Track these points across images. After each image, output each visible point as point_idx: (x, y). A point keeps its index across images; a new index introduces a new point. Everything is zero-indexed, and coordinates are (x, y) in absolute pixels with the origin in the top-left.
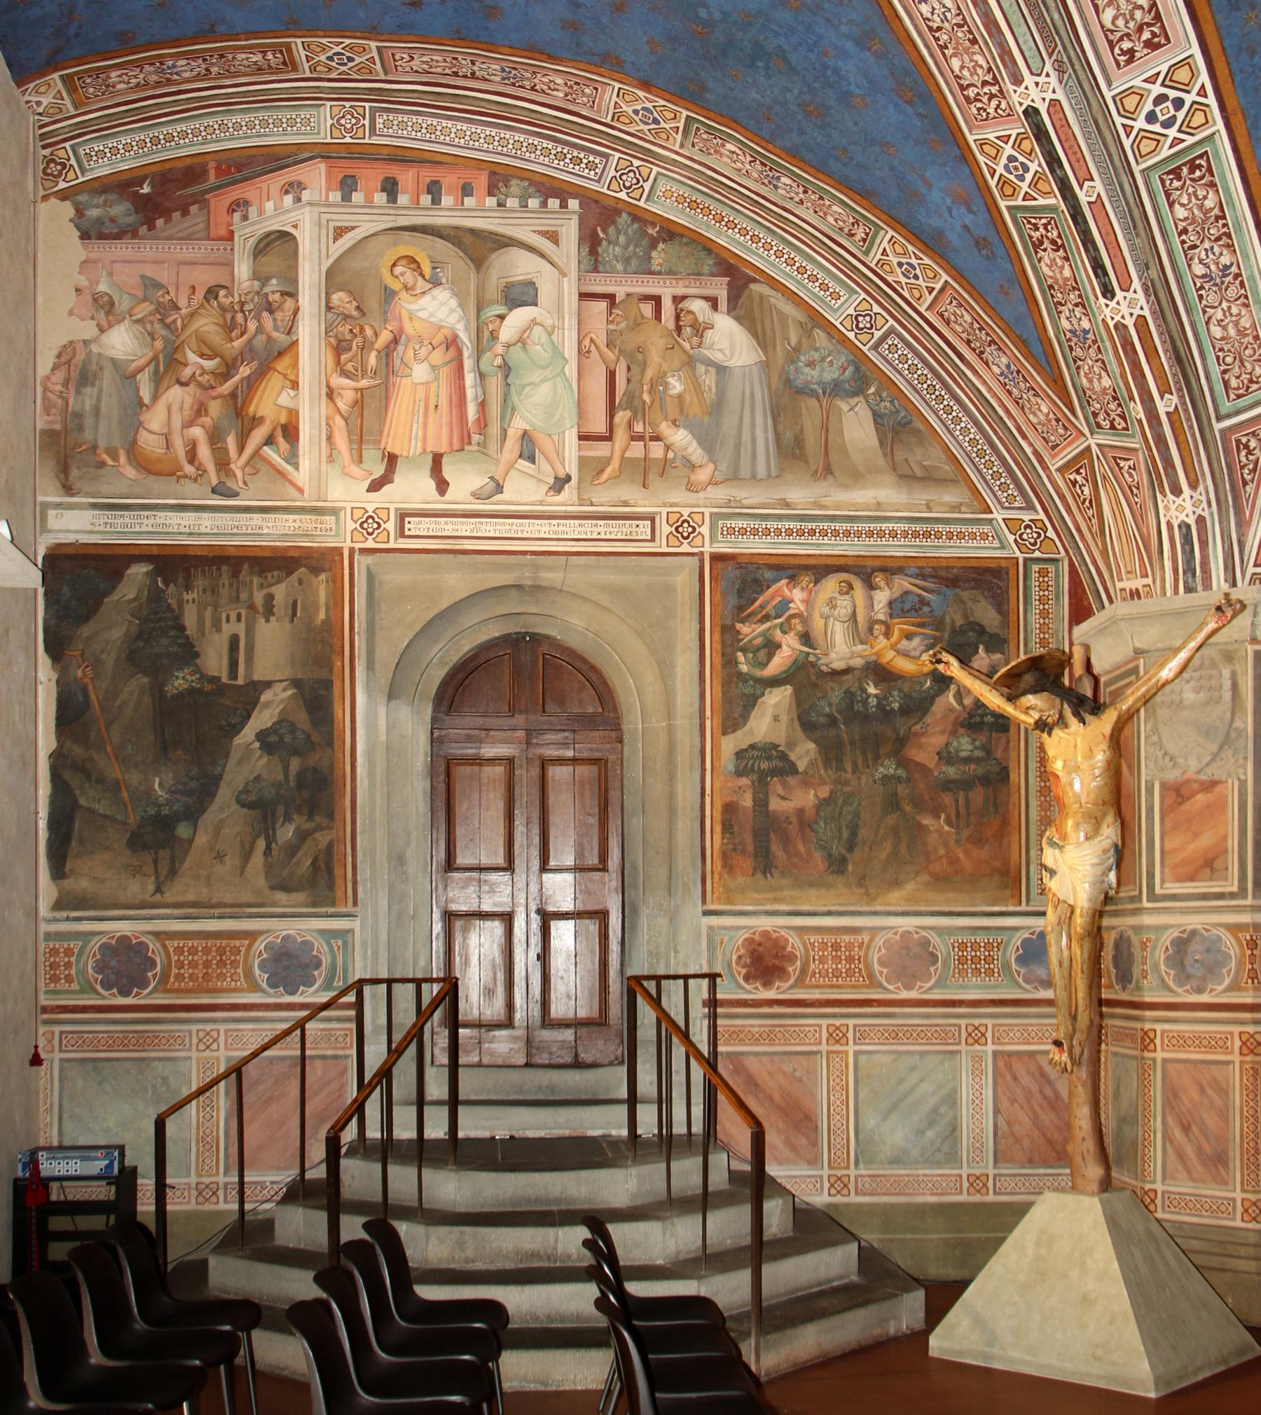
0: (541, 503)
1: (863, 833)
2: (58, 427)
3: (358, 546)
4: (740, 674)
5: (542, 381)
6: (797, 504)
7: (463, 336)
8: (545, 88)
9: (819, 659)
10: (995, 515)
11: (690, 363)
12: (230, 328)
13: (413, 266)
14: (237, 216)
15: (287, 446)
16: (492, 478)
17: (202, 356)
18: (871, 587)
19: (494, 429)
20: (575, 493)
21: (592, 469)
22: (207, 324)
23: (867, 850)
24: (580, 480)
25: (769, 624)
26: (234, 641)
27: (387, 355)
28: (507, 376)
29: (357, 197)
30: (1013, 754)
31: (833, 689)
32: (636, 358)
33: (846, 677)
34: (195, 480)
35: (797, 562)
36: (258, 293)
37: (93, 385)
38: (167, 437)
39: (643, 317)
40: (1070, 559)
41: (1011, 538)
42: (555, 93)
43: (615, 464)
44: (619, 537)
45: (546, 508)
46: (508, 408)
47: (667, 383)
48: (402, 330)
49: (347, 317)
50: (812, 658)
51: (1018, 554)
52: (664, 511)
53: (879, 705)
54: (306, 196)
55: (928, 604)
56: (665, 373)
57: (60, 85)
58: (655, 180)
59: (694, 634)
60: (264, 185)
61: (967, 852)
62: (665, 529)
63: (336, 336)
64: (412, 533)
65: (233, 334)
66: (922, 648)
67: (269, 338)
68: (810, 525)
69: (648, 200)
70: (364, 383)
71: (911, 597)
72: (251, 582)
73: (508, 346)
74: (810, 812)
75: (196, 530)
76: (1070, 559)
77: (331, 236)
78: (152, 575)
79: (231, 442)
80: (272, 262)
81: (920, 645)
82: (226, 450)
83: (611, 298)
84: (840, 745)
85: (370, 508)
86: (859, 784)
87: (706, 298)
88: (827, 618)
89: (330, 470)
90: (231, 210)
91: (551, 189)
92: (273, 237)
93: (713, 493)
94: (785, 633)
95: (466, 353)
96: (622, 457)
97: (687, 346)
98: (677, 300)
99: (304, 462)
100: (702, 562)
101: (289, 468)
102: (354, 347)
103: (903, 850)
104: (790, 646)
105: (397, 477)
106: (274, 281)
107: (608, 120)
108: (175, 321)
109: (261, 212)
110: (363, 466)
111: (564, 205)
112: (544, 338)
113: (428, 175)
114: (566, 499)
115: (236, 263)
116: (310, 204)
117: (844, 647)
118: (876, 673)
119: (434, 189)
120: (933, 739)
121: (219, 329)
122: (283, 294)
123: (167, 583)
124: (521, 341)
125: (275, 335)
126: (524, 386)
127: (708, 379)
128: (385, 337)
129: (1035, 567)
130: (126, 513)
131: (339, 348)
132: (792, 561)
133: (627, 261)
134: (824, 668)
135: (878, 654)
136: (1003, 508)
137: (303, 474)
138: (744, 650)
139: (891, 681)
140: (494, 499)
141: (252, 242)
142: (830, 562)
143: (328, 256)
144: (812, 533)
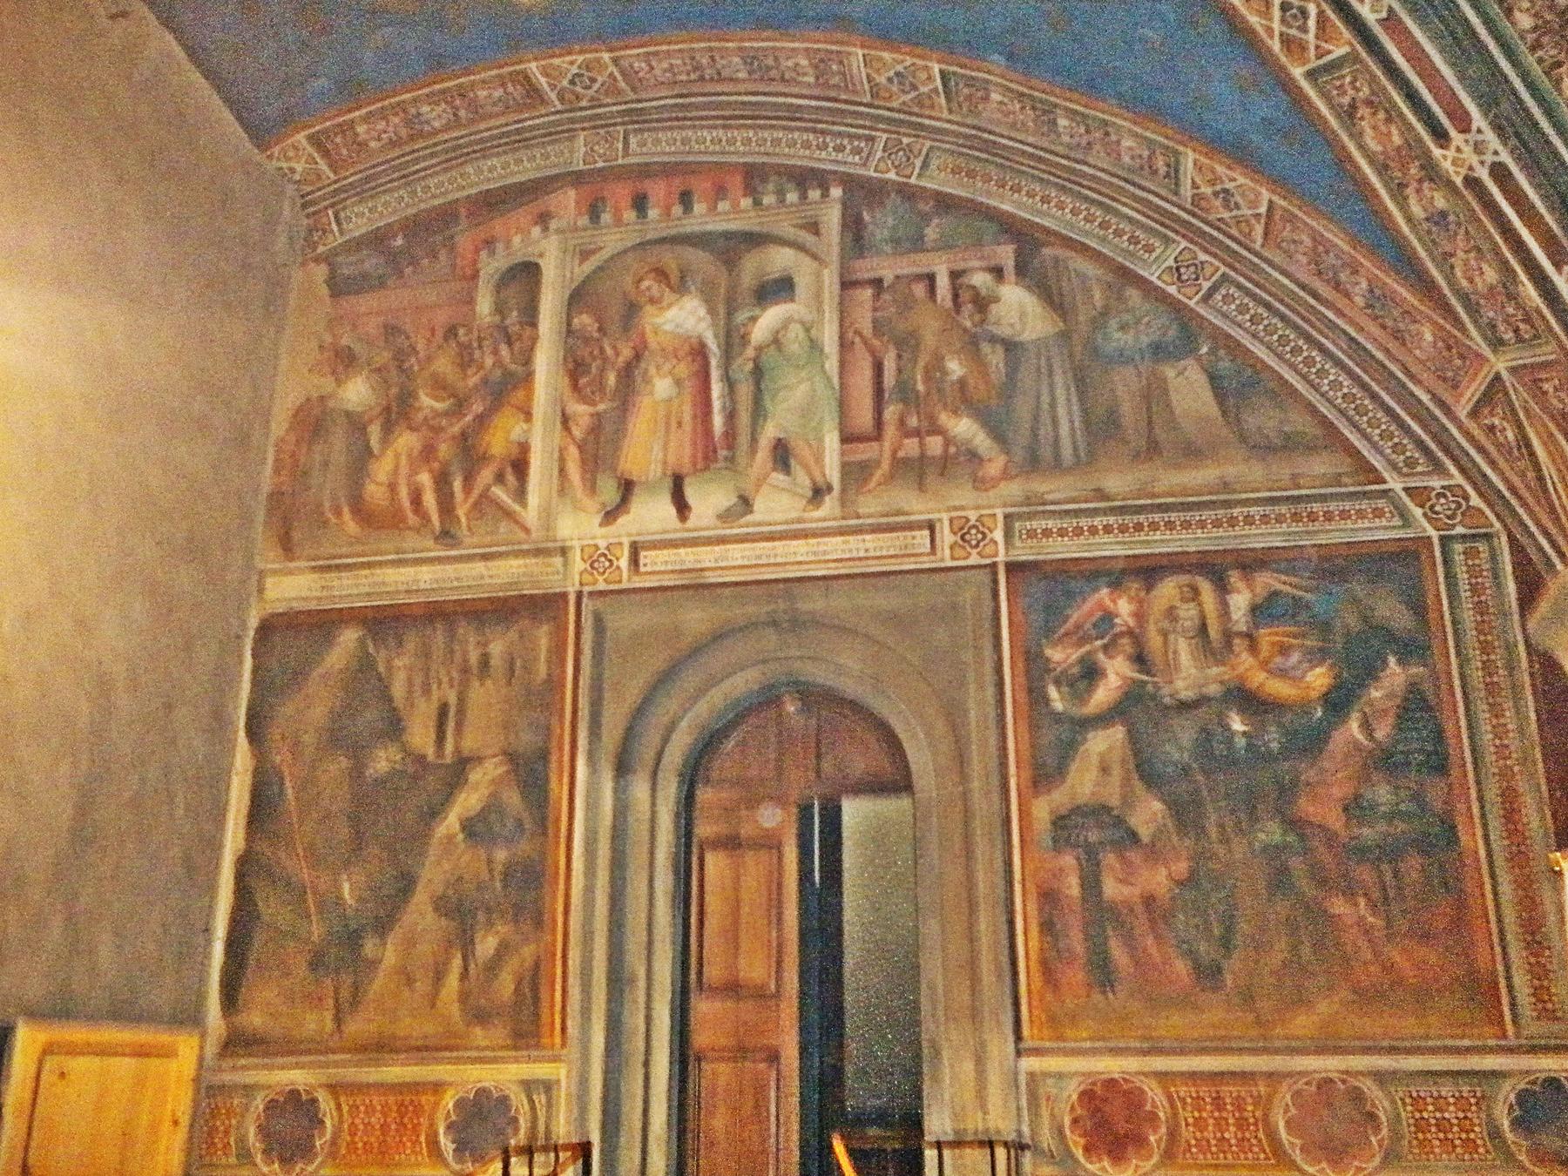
3: (587, 589)
8: (794, 75)
15: (516, 483)
17: (436, 398)
19: (743, 440)
20: (837, 503)
21: (856, 474)
22: (444, 365)
24: (843, 491)
29: (606, 218)
30: (1461, 807)
32: (907, 344)
34: (418, 531)
38: (392, 487)
41: (1418, 512)
42: (806, 79)
43: (886, 465)
47: (945, 373)
50: (1150, 688)
53: (1250, 747)
54: (553, 225)
55: (1308, 607)
57: (310, 149)
58: (927, 155)
62: (946, 537)
64: (649, 569)
65: (469, 372)
69: (920, 175)
70: (601, 407)
79: (457, 485)
82: (452, 494)
83: (877, 283)
85: (602, 544)
91: (805, 178)
95: (714, 362)
97: (968, 324)
99: (534, 498)
100: (995, 574)
101: (517, 508)
102: (594, 370)
104: (1117, 672)
107: (867, 99)
108: (412, 366)
111: (825, 194)
112: (802, 335)
113: (677, 184)
116: (559, 231)
117: (1193, 671)
124: (776, 341)
126: (779, 390)
127: (995, 358)
128: (627, 353)
129: (1458, 547)
133: (896, 241)
134: (1167, 700)
135: (1241, 677)
137: (531, 513)
140: (743, 521)
144: (1139, 527)
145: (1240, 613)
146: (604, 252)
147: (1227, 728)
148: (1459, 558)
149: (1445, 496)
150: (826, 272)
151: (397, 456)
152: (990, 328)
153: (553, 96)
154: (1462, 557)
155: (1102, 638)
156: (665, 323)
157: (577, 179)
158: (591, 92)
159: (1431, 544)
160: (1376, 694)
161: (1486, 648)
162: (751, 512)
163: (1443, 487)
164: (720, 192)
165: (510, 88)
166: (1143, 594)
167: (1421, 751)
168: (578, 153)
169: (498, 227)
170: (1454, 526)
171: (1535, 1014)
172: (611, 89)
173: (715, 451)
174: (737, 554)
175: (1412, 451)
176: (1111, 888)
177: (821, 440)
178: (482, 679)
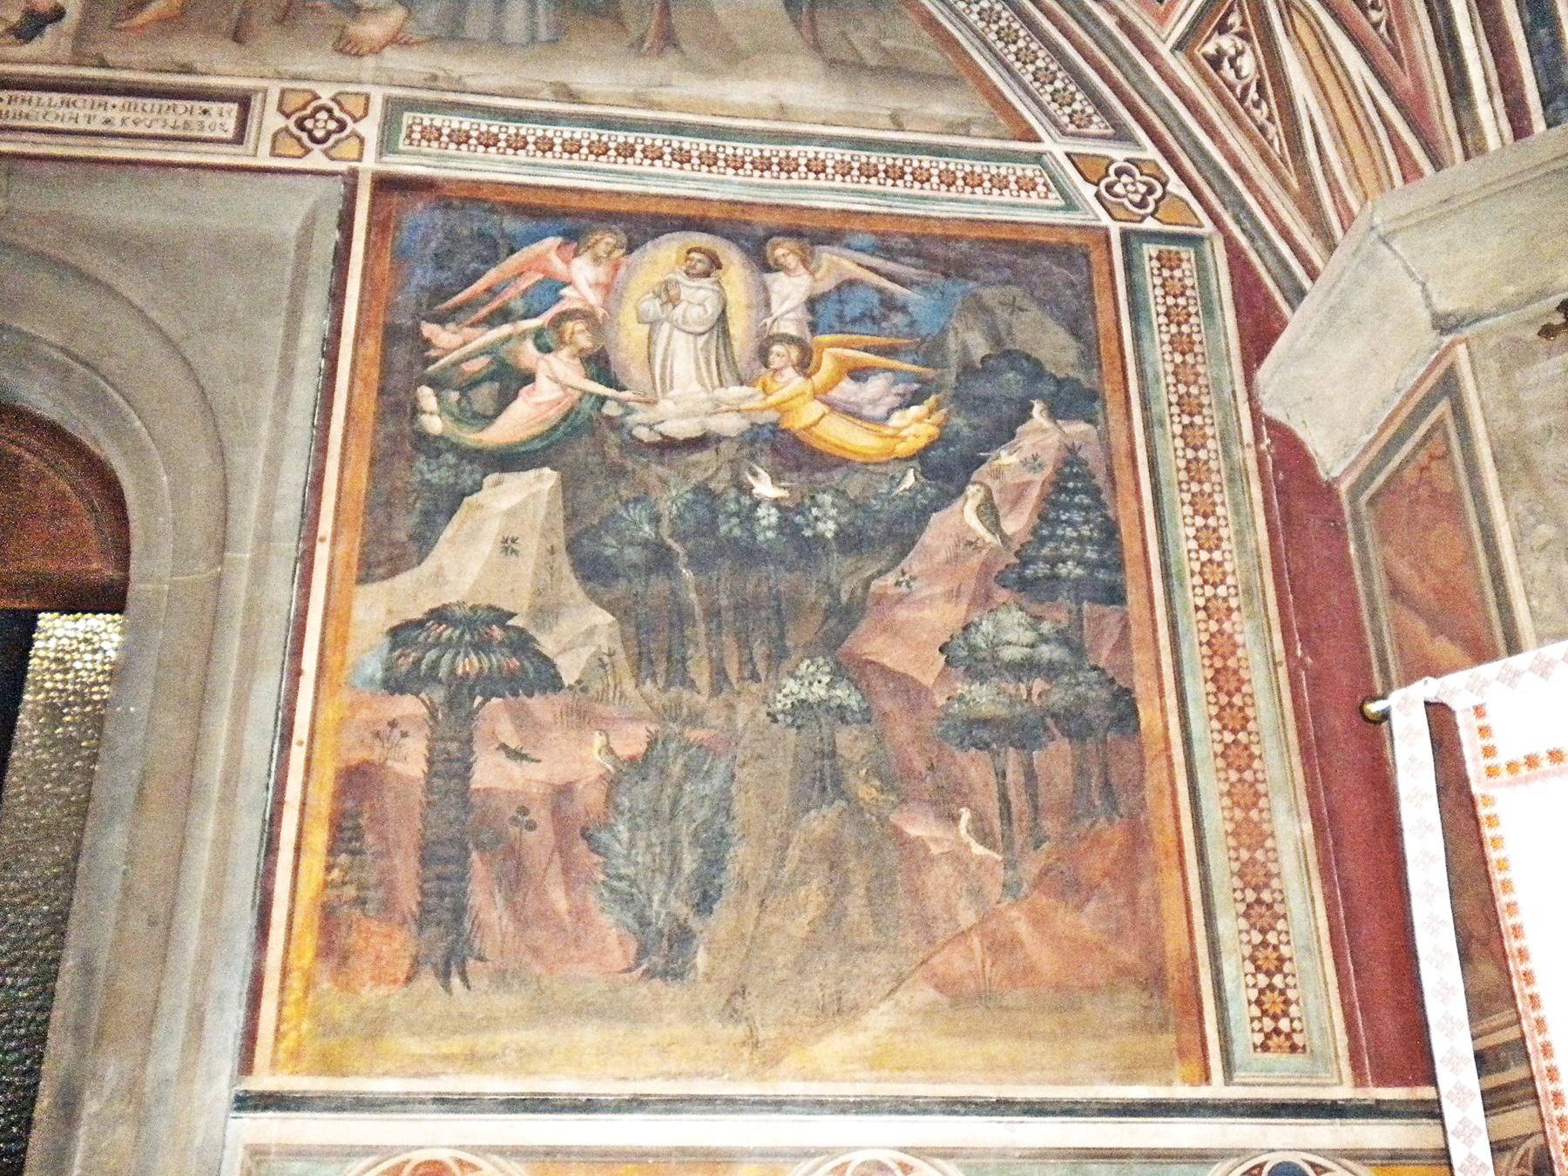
1: (741, 857)
6: (592, 96)
9: (629, 411)
10: (1047, 145)
18: (766, 266)
23: (752, 906)
25: (506, 329)
30: (1140, 658)
31: (664, 482)
33: (696, 457)
35: (587, 203)
40: (1230, 242)
41: (1089, 191)
50: (611, 409)
51: (1105, 220)
55: (903, 309)
61: (1039, 921)
66: (892, 400)
71: (860, 293)
74: (591, 796)
76: (1230, 242)
81: (888, 393)
84: (680, 616)
86: (729, 719)
88: (654, 324)
93: (394, 59)
94: (545, 349)
103: (855, 906)
117: (696, 387)
118: (775, 451)
120: (927, 613)
129: (1150, 250)
132: (574, 202)
134: (643, 434)
136: (1064, 134)
138: (437, 384)
139: (815, 469)
142: (665, 208)
144: (627, 151)
145: (788, 305)
147: (744, 489)
148: (1149, 266)
149: (1131, 175)
154: (1155, 264)
155: (536, 315)
159: (1108, 238)
160: (1006, 458)
161: (1186, 405)
163: (1128, 160)
166: (618, 253)
167: (1081, 562)
170: (1143, 218)
171: (1259, 1038)
175: (1080, 103)
176: (489, 772)
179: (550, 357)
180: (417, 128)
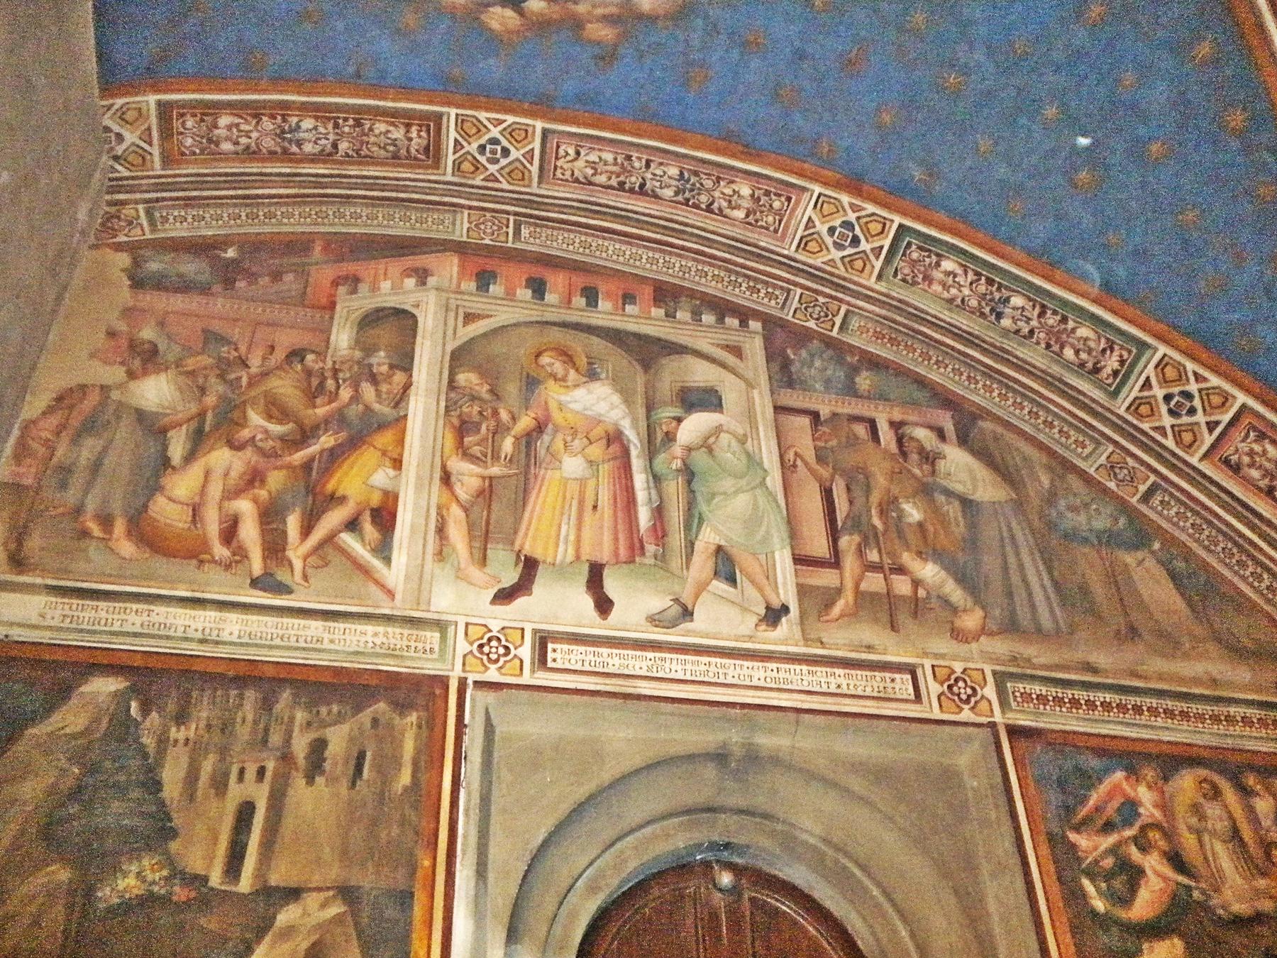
0: (750, 638)
2: (28, 481)
4: (1094, 913)
5: (736, 492)
7: (630, 434)
11: (926, 491)
12: (313, 394)
13: (565, 358)
14: (342, 290)
16: (676, 600)
17: (270, 417)
19: (676, 539)
22: (285, 387)
24: (803, 616)
26: (245, 813)
27: (528, 445)
28: (689, 482)
32: (858, 479)
34: (228, 567)
36: (359, 363)
37: (98, 435)
38: (196, 512)
39: (857, 438)
43: (848, 597)
44: (868, 692)
45: (758, 646)
46: (693, 520)
47: (902, 510)
48: (548, 419)
49: (474, 398)
52: (927, 664)
54: (432, 281)
56: (896, 498)
58: (846, 315)
59: (1008, 844)
60: (382, 267)
63: (460, 416)
64: (558, 665)
65: (318, 401)
67: (368, 408)
68: (1133, 700)
70: (495, 470)
72: (292, 719)
73: (689, 449)
75: (214, 637)
77: (461, 319)
78: (121, 699)
79: (293, 523)
80: (385, 334)
83: (815, 416)
85: (495, 626)
87: (931, 428)
89: (437, 571)
90: (336, 283)
92: (386, 312)
96: (857, 591)
97: (917, 471)
98: (896, 426)
99: (400, 556)
101: (376, 563)
105: (537, 588)
106: (382, 354)
109: (374, 288)
110: (487, 570)
111: (744, 323)
114: (785, 636)
115: (334, 330)
119: (591, 296)
121: (302, 395)
122: (392, 367)
123: (145, 711)
124: (706, 445)
125: (376, 407)
126: (713, 495)
127: (953, 510)
128: (525, 422)
130: (102, 604)
131: (463, 429)
137: (397, 572)
141: (356, 315)
143: (455, 338)
144: (1138, 710)
146: (492, 320)
150: (756, 393)
151: (207, 474)
152: (944, 483)
153: (451, 158)
155: (1131, 825)
156: (570, 402)
157: (460, 248)
158: (493, 168)
162: (692, 621)
164: (628, 298)
165: (414, 134)
168: (460, 229)
169: (365, 269)
172: (517, 173)
173: (642, 548)
174: (676, 666)
177: (770, 555)
178: (310, 780)
179: (1148, 857)
180: (1018, 694)
